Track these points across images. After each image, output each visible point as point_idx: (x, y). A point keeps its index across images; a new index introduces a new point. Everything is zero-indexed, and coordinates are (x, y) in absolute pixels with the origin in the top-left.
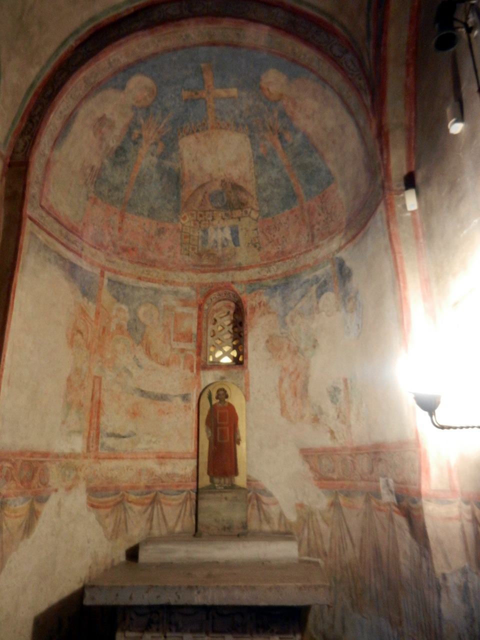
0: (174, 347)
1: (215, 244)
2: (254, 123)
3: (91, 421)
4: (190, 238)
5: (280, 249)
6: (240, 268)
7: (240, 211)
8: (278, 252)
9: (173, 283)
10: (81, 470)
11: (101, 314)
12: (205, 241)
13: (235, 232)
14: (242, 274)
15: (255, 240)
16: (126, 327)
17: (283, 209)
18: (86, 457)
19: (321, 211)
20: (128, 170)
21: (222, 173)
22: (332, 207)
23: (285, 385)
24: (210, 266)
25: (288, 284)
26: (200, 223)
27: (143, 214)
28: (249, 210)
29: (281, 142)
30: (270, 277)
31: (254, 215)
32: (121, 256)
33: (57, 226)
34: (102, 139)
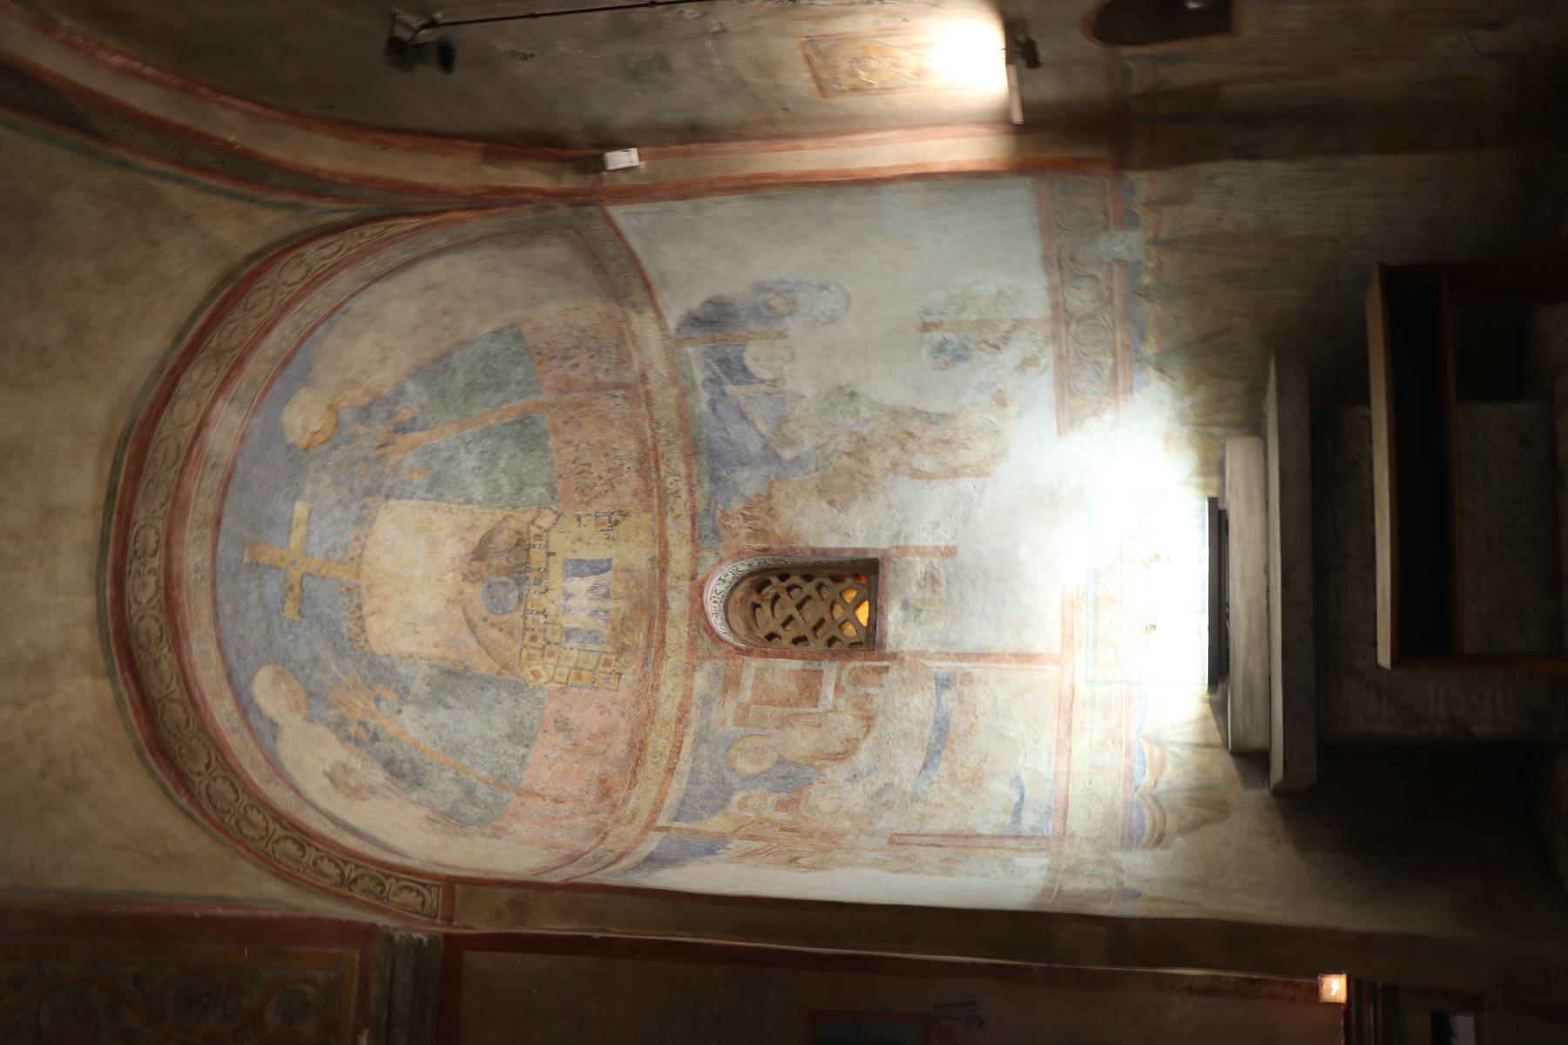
0: (831, 708)
1: (601, 613)
2: (367, 483)
4: (581, 669)
5: (631, 464)
6: (662, 562)
7: (532, 550)
8: (638, 471)
9: (684, 709)
12: (594, 636)
13: (578, 568)
14: (674, 556)
15: (602, 524)
16: (783, 796)
17: (545, 450)
19: (572, 362)
20: (430, 764)
21: (449, 577)
22: (570, 334)
24: (650, 628)
25: (711, 450)
26: (549, 643)
27: (523, 756)
28: (534, 530)
29: (412, 429)
30: (691, 493)
31: (546, 520)
32: (619, 803)
34: (372, 791)
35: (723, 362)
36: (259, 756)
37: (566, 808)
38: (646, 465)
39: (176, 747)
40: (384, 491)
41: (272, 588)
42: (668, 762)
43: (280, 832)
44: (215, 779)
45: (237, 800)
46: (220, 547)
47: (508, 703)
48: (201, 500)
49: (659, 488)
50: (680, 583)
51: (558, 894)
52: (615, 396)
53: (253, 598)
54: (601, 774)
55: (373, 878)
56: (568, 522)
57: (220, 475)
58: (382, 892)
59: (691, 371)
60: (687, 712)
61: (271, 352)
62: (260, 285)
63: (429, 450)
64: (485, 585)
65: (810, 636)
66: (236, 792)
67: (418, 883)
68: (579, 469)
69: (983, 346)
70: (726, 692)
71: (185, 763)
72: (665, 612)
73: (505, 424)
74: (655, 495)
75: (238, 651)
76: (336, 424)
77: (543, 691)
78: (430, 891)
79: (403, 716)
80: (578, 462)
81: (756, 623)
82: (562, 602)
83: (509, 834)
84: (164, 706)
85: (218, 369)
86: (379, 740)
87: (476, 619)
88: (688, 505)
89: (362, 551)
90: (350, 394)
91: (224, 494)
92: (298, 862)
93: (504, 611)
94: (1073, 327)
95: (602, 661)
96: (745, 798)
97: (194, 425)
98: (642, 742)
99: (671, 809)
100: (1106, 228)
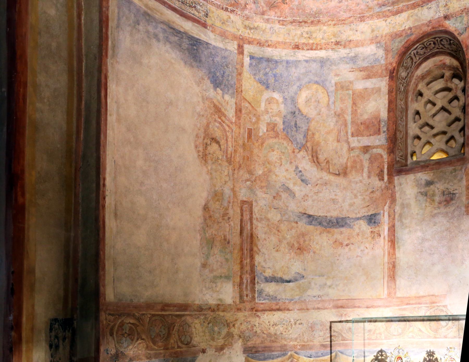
0: (352, 145)
3: (241, 261)
9: (347, 44)
10: (234, 326)
11: (243, 111)
16: (281, 126)
18: (239, 310)
32: (266, 17)
42: (303, 44)
50: (442, 9)
60: (344, 47)
70: (361, 71)
81: (431, 82)
96: (277, 102)
98: (319, 21)
99: (262, 53)
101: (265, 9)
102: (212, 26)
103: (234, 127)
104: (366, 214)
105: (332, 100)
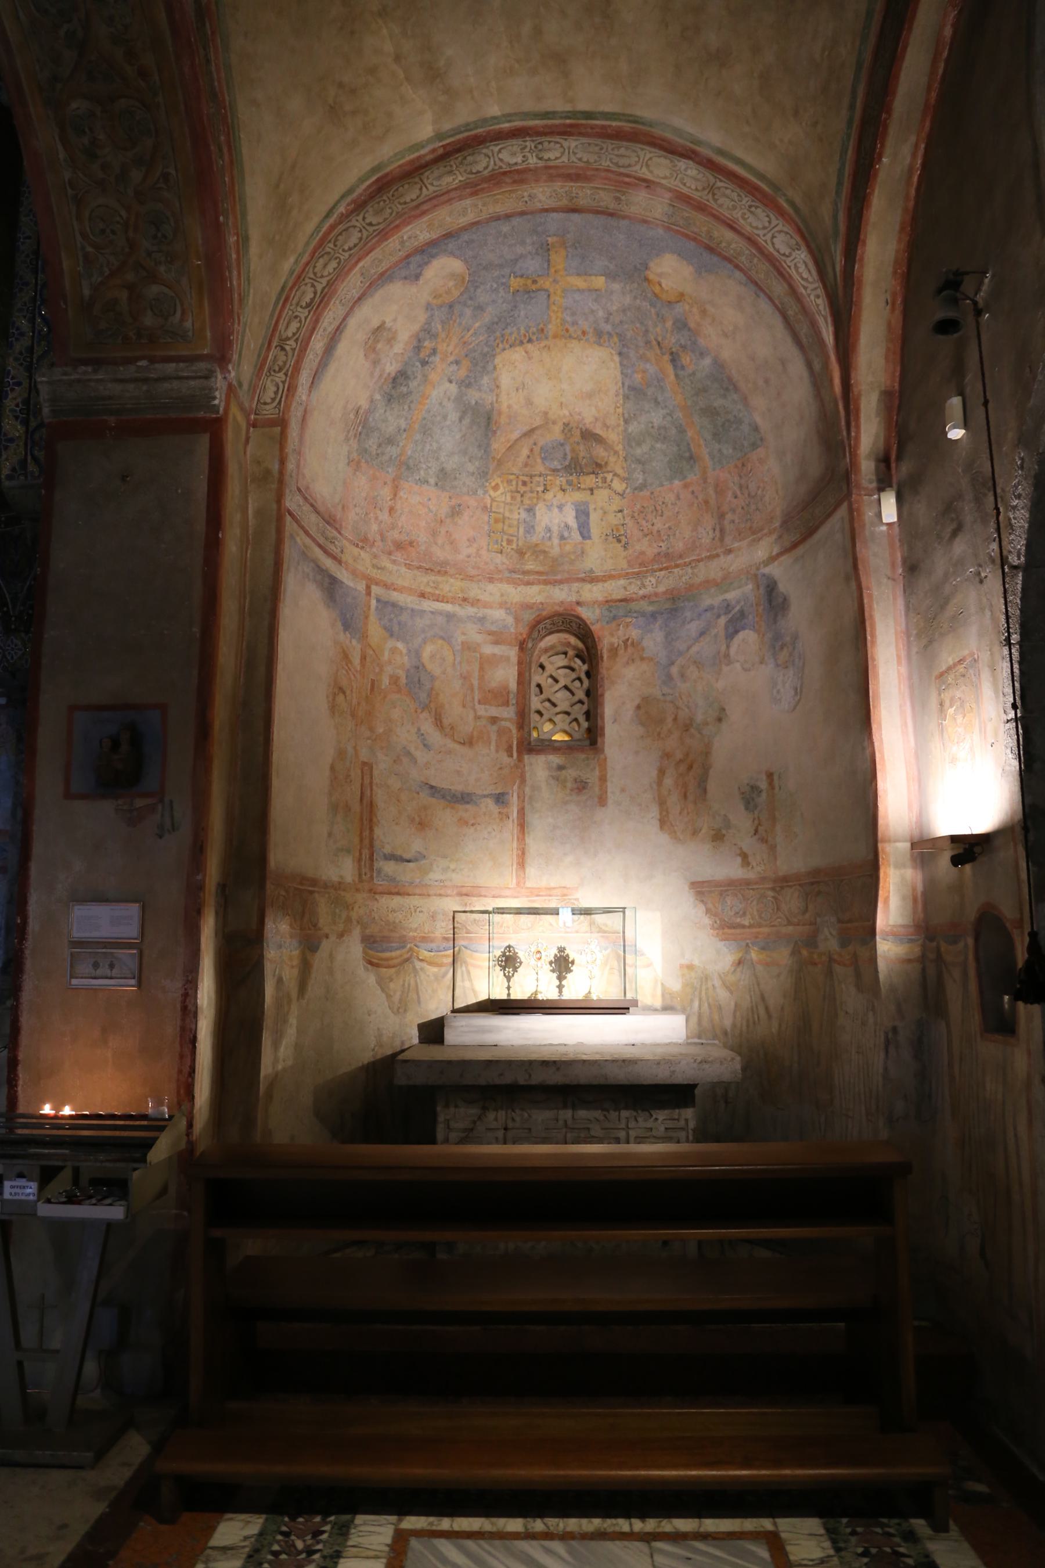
1: (548, 535)
2: (629, 334)
3: (361, 833)
4: (504, 522)
5: (664, 548)
6: (592, 579)
8: (659, 554)
9: (475, 602)
10: (353, 909)
11: (368, 659)
12: (530, 529)
13: (583, 514)
14: (595, 588)
15: (618, 530)
16: (403, 681)
17: (671, 479)
18: (358, 890)
19: (738, 492)
22: (758, 488)
23: (668, 782)
25: (676, 610)
27: (428, 482)
28: (609, 476)
29: (675, 367)
30: (644, 597)
31: (618, 485)
32: (393, 558)
33: (314, 518)
34: (376, 362)
35: (742, 614)
36: (384, 266)
37: (384, 516)
38: (664, 560)
39: (385, 198)
40: (625, 350)
41: (532, 265)
43: (319, 287)
44: (361, 231)
45: (344, 250)
46: (555, 215)
47: (471, 467)
48: (589, 192)
49: (647, 572)
51: (274, 506)
52: (714, 530)
53: (519, 250)
54: (418, 543)
55: (285, 363)
56: (617, 503)
57: (612, 206)
58: (274, 371)
59: (734, 589)
61: (716, 234)
62: (772, 216)
63: (662, 384)
64: (562, 441)
65: (543, 697)
66: (350, 249)
67: (281, 397)
68: (658, 508)
69: (756, 822)
71: (372, 206)
72: (551, 583)
73: (689, 444)
74: (641, 568)
75: (472, 241)
76: (669, 302)
77: (484, 494)
78: (276, 407)
79: (448, 385)
80: (664, 506)
82: (555, 503)
83: (355, 474)
84: (416, 183)
85: (697, 190)
86: (422, 366)
87: (535, 437)
88: (634, 596)
89: (575, 339)
90: (695, 310)
91: (597, 212)
92: (297, 304)
93: (544, 459)
94: (771, 893)
95: (511, 538)
96: (401, 653)
97: (649, 176)
98: (446, 572)
100: (840, 921)
101: (392, 548)
102: (346, 563)
103: (358, 676)
104: (494, 792)
105: (458, 659)
